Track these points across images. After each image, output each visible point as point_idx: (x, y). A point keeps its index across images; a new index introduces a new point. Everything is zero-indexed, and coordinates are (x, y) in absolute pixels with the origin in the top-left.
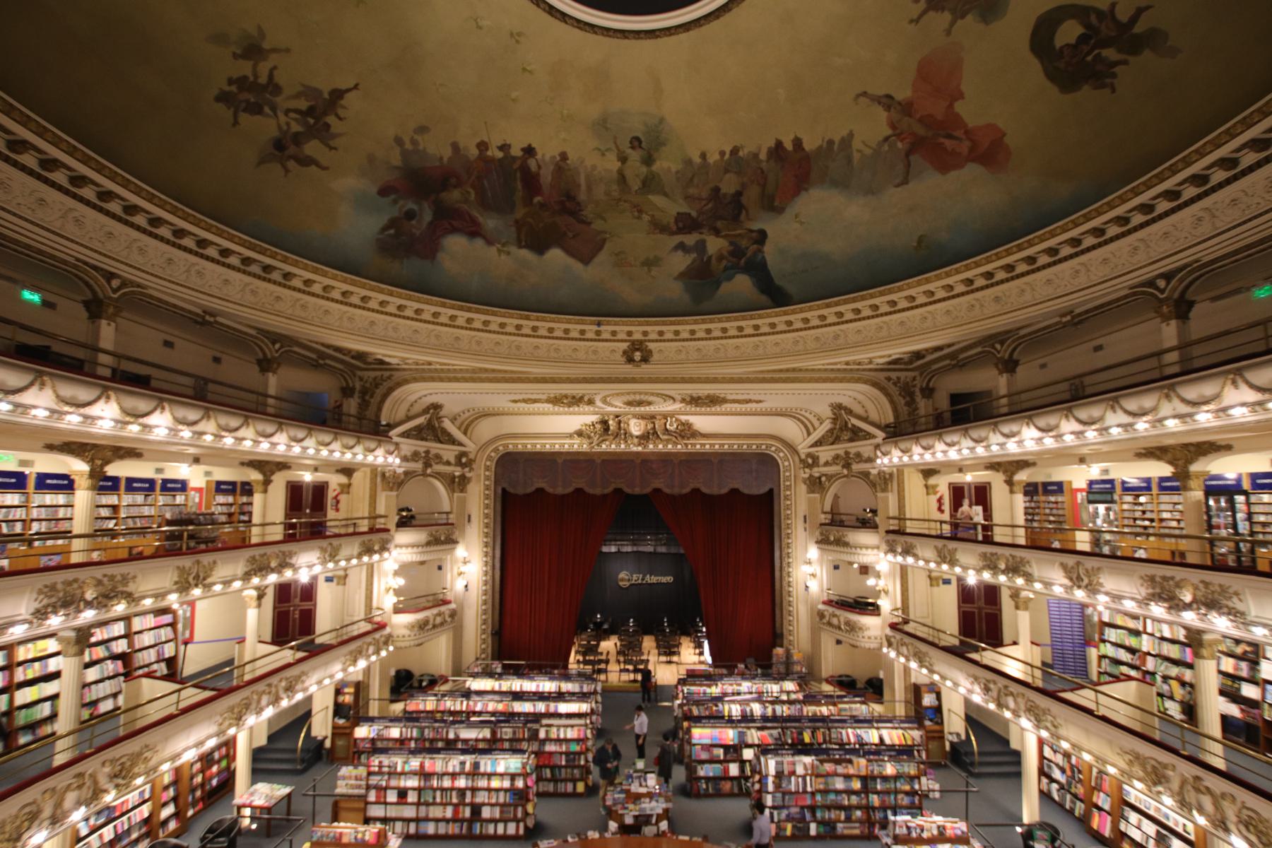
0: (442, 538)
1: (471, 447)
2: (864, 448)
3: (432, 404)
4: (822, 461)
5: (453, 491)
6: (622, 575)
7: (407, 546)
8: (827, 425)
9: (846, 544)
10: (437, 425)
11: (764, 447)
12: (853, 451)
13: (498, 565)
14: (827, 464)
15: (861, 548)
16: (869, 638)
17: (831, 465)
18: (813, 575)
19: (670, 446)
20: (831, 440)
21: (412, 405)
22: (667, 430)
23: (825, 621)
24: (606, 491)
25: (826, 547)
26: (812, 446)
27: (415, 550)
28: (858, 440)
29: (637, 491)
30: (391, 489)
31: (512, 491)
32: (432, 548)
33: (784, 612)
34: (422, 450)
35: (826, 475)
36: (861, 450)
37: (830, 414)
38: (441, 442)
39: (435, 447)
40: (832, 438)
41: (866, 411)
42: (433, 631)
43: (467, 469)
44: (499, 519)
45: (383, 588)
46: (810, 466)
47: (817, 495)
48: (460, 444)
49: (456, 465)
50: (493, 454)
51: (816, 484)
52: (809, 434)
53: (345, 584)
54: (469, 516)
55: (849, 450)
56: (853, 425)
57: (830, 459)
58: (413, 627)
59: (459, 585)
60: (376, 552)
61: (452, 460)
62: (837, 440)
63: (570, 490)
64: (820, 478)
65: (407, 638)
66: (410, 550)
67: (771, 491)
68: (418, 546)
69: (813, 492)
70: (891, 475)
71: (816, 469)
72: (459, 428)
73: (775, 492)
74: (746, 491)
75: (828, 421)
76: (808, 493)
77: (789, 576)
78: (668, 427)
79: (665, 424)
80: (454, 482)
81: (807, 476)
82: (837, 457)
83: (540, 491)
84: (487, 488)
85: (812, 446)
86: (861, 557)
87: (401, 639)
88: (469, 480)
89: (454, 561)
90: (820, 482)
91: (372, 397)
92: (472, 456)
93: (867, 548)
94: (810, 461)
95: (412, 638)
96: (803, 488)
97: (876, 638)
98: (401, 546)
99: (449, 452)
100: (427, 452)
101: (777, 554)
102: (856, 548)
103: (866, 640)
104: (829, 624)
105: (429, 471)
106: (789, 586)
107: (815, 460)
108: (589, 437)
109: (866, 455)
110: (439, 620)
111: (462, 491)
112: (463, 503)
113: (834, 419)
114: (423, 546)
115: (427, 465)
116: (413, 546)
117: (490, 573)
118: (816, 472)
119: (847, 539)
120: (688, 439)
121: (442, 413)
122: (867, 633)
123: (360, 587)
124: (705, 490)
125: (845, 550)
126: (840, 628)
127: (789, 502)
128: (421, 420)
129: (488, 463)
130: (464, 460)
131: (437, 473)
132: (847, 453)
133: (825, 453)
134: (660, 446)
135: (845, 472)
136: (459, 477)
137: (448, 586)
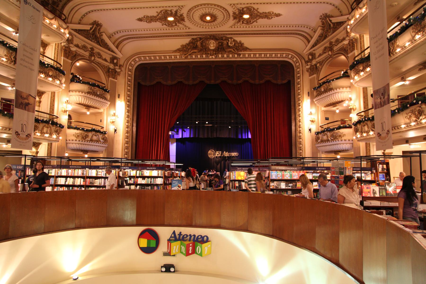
0: (98, 93)
1: (119, 55)
2: (339, 34)
3: (95, 22)
4: (317, 55)
5: (109, 77)
6: (209, 152)
7: (76, 91)
8: (319, 31)
9: (331, 89)
10: (98, 36)
11: (284, 55)
12: (333, 40)
13: (135, 125)
14: (320, 55)
15: (339, 88)
16: (345, 140)
17: (322, 55)
18: (312, 121)
19: (231, 56)
20: (322, 40)
21: (82, 18)
22: (229, 46)
23: (319, 141)
24: (195, 83)
25: (320, 97)
26: (311, 48)
27: (80, 94)
28: (336, 31)
29: (213, 82)
30: (68, 59)
31: (143, 83)
32: (91, 96)
33: (297, 148)
34: (89, 46)
35: (318, 63)
36: (338, 37)
37: (320, 24)
38: (101, 46)
39: (98, 48)
40: (323, 37)
41: (341, 12)
42: (90, 143)
43: (116, 67)
44: (136, 99)
45: (60, 109)
46: (310, 61)
47: (315, 75)
48: (112, 51)
49: (111, 63)
50: (133, 63)
51: (314, 70)
52: (309, 42)
53: (39, 106)
54: (119, 95)
55: (332, 41)
56: (334, 24)
57: (321, 52)
58: (78, 136)
59: (111, 128)
60: (50, 76)
61: (109, 60)
62: (326, 37)
63: (174, 83)
64: (316, 65)
65: (74, 142)
66: (77, 93)
67: (289, 82)
68: (82, 92)
69: (313, 74)
70: (356, 40)
71: (314, 60)
72: (114, 44)
73: (292, 82)
74: (274, 82)
75: (320, 28)
76: (310, 76)
77: (300, 122)
78: (229, 44)
79: (228, 43)
80: (109, 71)
81: (308, 67)
82: (325, 48)
83: (159, 83)
84: (129, 80)
85: (311, 48)
86: (339, 95)
87: (71, 142)
88: (119, 74)
89: (108, 115)
90: (316, 67)
91: (58, 6)
92: (121, 62)
93: (343, 88)
94: (310, 57)
95: (77, 142)
96: (306, 74)
97: (349, 140)
98: (72, 91)
99: (107, 55)
100: (92, 49)
101: (293, 117)
102: (336, 89)
103: (343, 142)
104: (322, 141)
105: (93, 58)
106: (300, 133)
107: (313, 55)
108: (185, 51)
109: (341, 38)
110: (95, 138)
111: (114, 78)
112: (114, 85)
113: (323, 27)
114: (85, 93)
115: (92, 54)
116: (79, 92)
117: (131, 127)
118: (314, 62)
119: (331, 87)
120: (241, 51)
121: (102, 30)
122: (343, 138)
123: (48, 105)
124: (252, 82)
125: (331, 93)
126: (328, 140)
127: (299, 86)
128: (88, 27)
129: (130, 68)
130: (115, 61)
131: (98, 63)
132: (331, 43)
133: (318, 50)
134: (225, 56)
135: (330, 53)
136: (113, 69)
137: (105, 126)
